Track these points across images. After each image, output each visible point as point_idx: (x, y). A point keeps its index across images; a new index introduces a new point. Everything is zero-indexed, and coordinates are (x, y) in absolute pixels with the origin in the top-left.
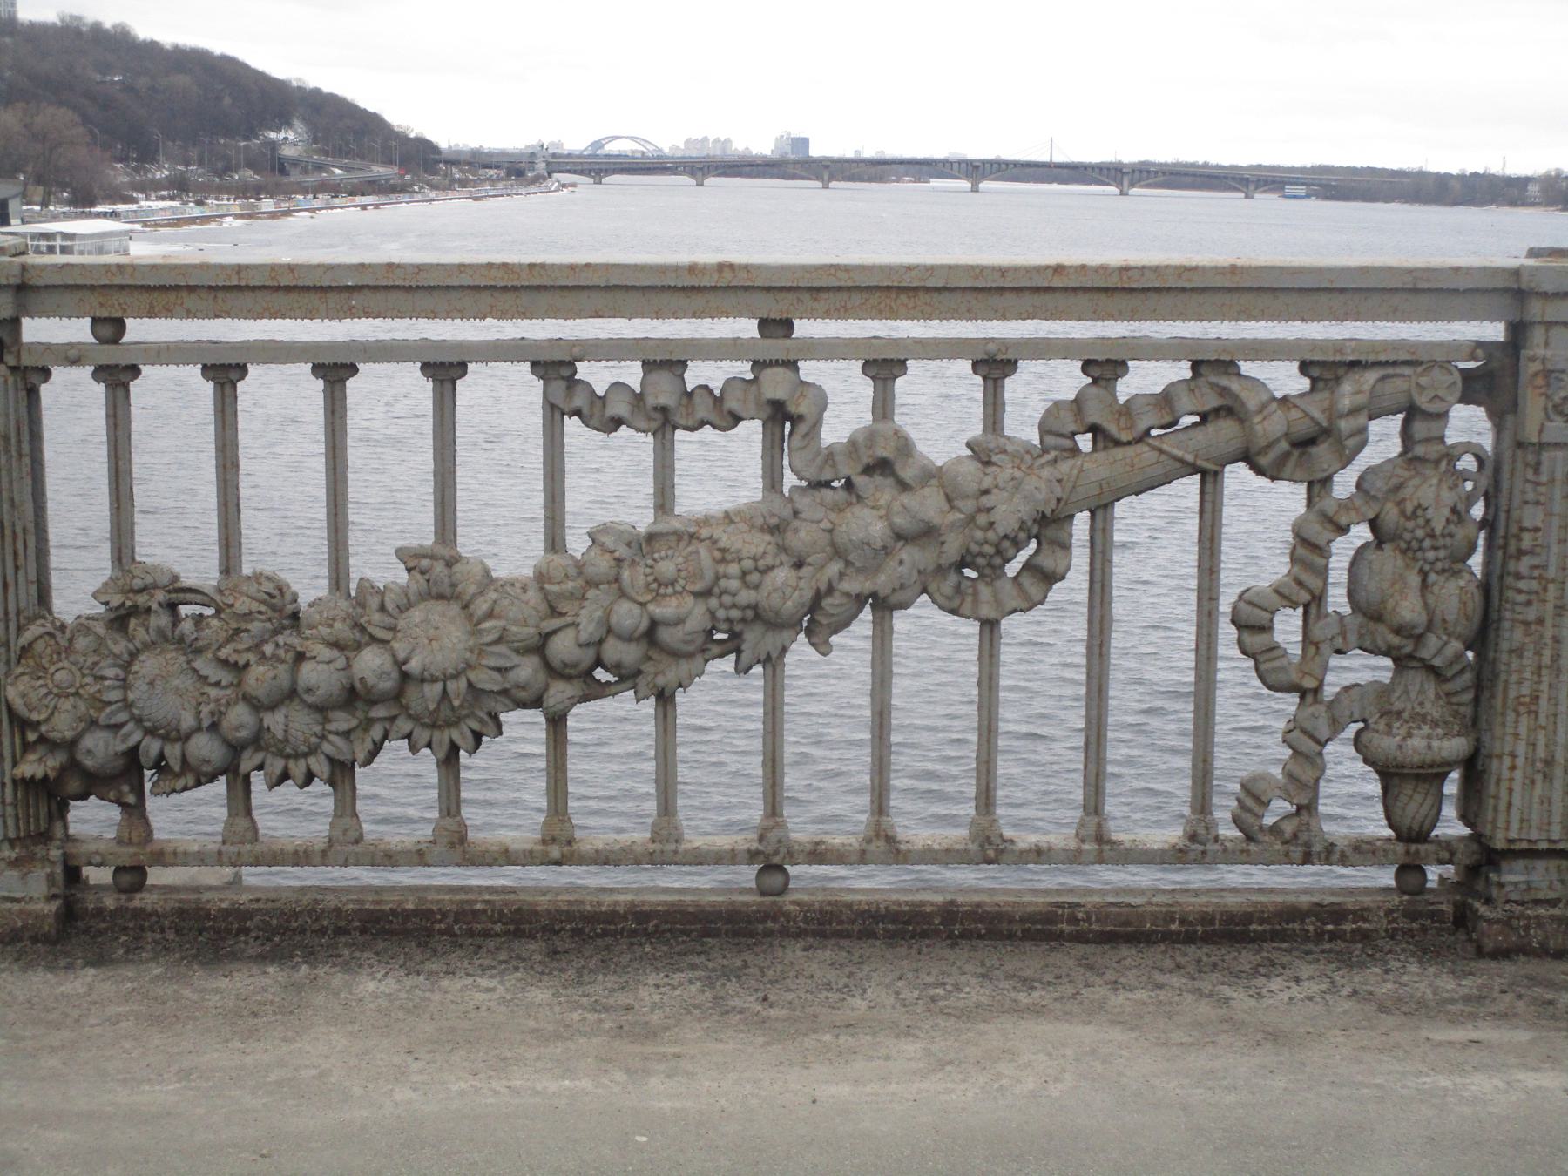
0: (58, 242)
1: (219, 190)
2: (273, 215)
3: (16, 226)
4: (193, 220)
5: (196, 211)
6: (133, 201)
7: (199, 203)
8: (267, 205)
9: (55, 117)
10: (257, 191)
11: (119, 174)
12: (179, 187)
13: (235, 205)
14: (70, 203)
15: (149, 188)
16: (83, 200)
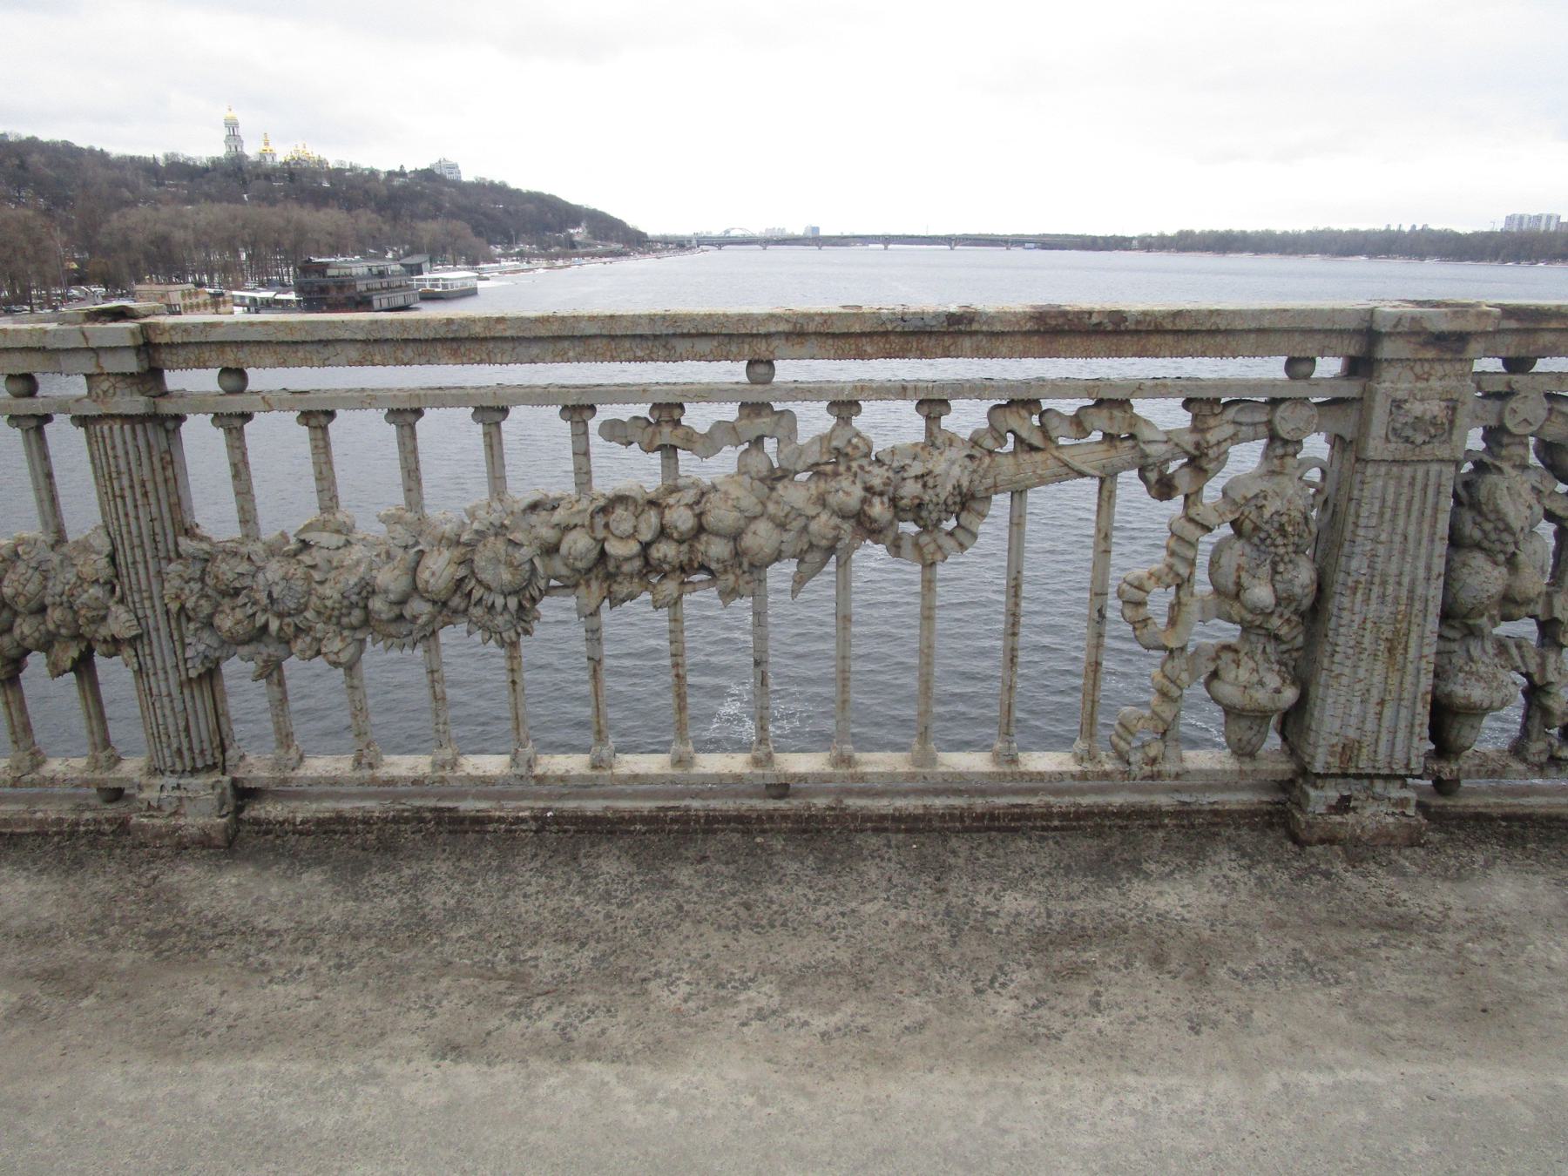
0: (441, 282)
1: (538, 256)
2: (561, 267)
3: (426, 275)
4: (523, 271)
5: (525, 266)
6: (499, 262)
7: (528, 262)
8: (560, 263)
9: (459, 226)
10: (557, 256)
11: (499, 250)
12: (521, 255)
13: (544, 263)
14: (468, 263)
15: (506, 256)
16: (473, 262)
